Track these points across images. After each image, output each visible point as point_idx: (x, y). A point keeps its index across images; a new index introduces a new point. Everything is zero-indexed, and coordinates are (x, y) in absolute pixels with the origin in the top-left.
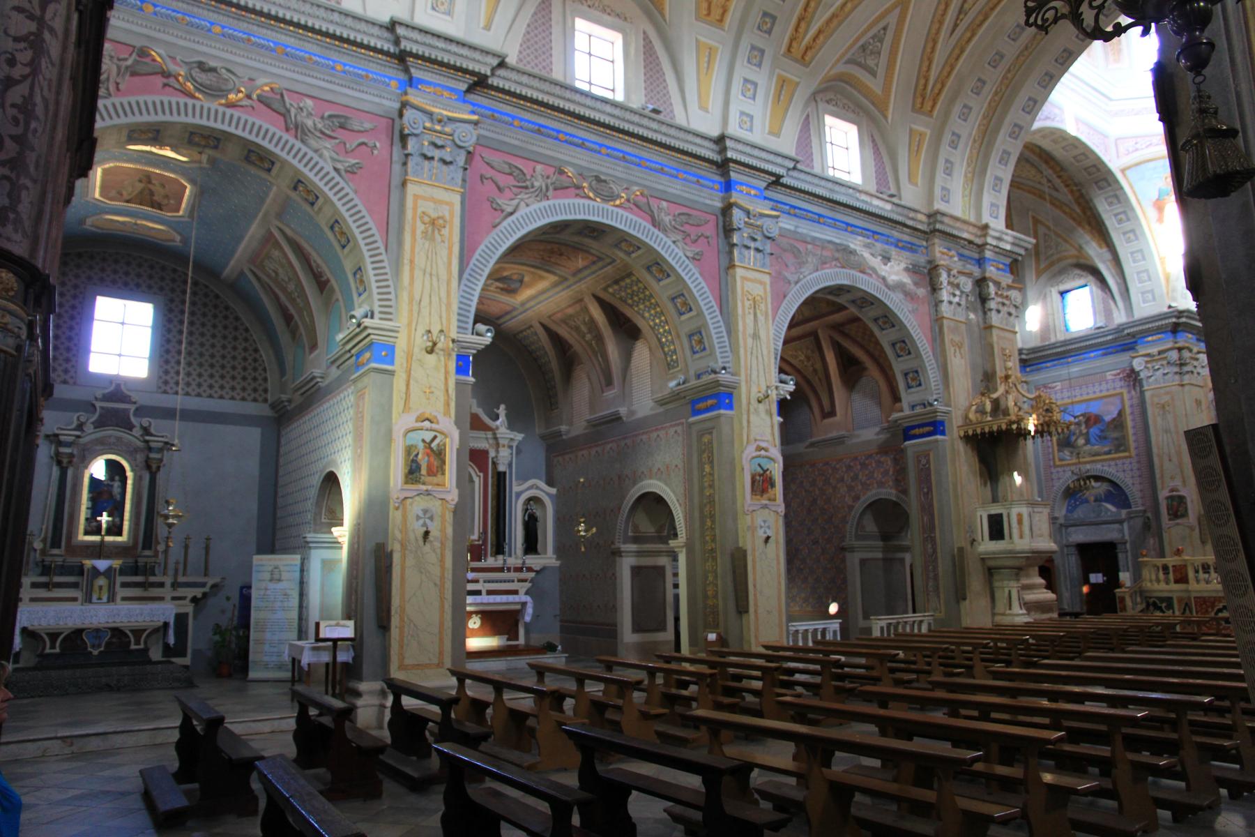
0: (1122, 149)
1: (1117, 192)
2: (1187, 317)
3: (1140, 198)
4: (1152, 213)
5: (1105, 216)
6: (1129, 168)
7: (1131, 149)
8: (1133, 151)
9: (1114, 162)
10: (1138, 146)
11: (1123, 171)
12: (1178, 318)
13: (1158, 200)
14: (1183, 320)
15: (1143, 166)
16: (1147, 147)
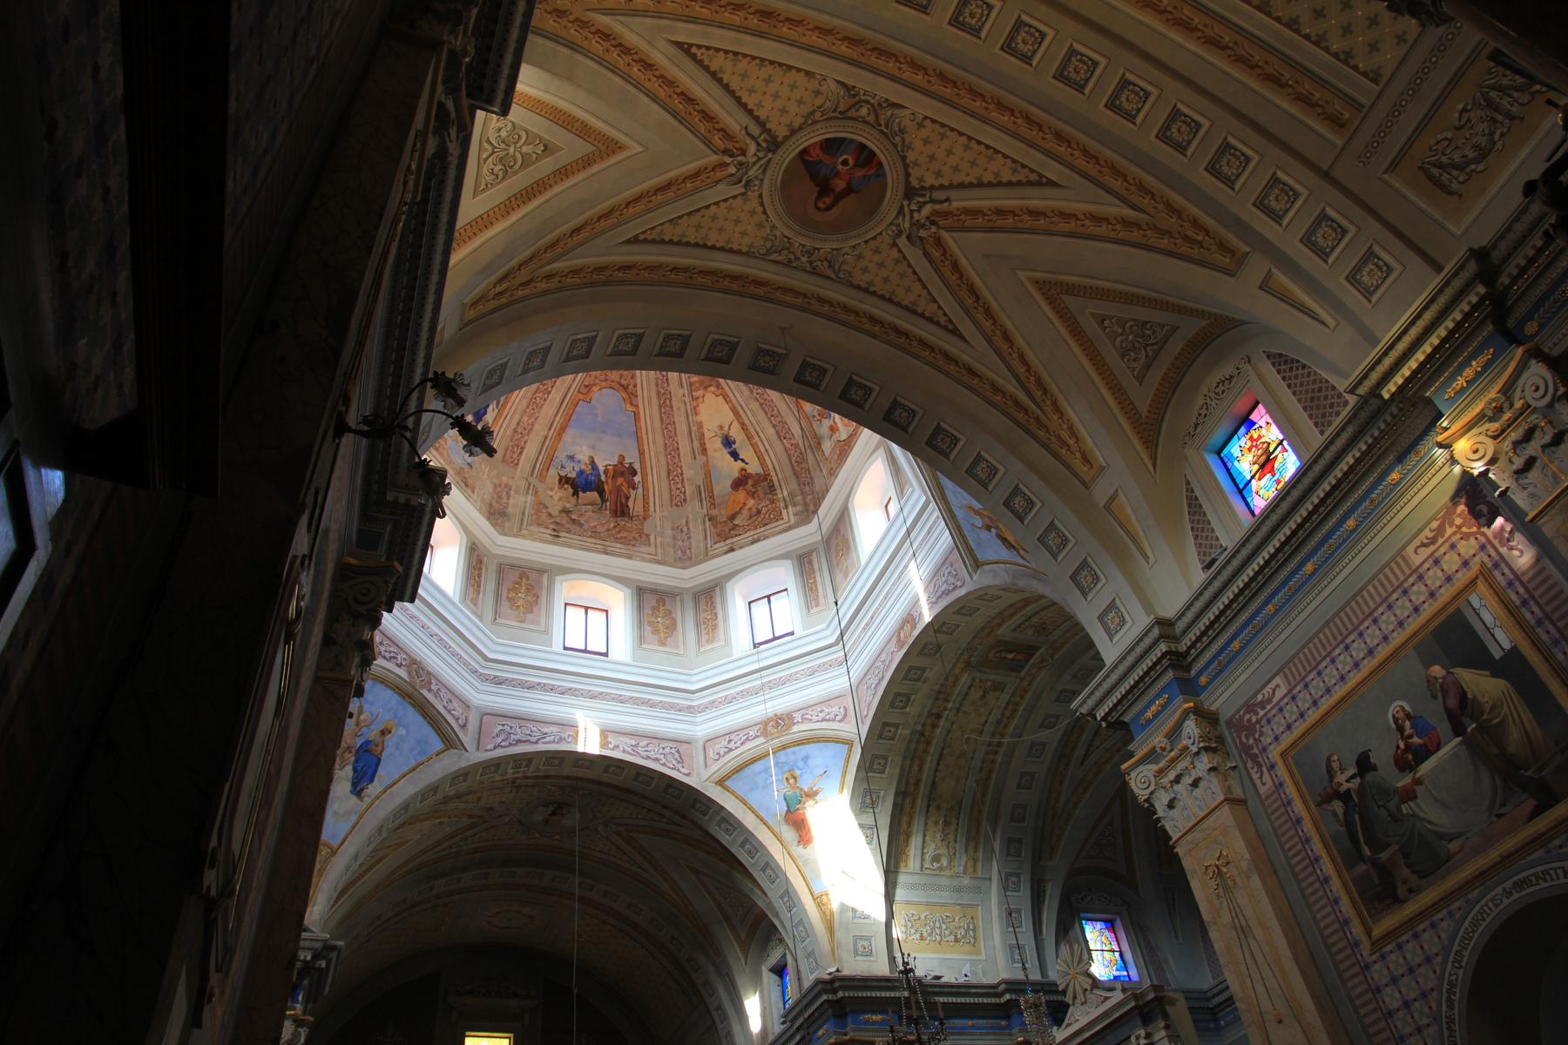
0: (711, 754)
1: (722, 814)
2: (843, 988)
3: (763, 815)
4: (789, 834)
5: (733, 850)
6: (728, 777)
7: (722, 753)
8: (726, 753)
9: (699, 776)
10: (732, 745)
11: (721, 783)
12: (835, 992)
13: (788, 811)
14: (840, 994)
15: (747, 771)
16: (742, 744)
